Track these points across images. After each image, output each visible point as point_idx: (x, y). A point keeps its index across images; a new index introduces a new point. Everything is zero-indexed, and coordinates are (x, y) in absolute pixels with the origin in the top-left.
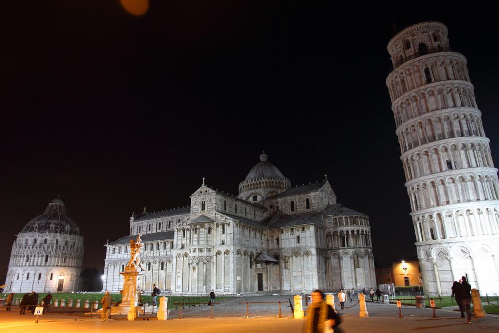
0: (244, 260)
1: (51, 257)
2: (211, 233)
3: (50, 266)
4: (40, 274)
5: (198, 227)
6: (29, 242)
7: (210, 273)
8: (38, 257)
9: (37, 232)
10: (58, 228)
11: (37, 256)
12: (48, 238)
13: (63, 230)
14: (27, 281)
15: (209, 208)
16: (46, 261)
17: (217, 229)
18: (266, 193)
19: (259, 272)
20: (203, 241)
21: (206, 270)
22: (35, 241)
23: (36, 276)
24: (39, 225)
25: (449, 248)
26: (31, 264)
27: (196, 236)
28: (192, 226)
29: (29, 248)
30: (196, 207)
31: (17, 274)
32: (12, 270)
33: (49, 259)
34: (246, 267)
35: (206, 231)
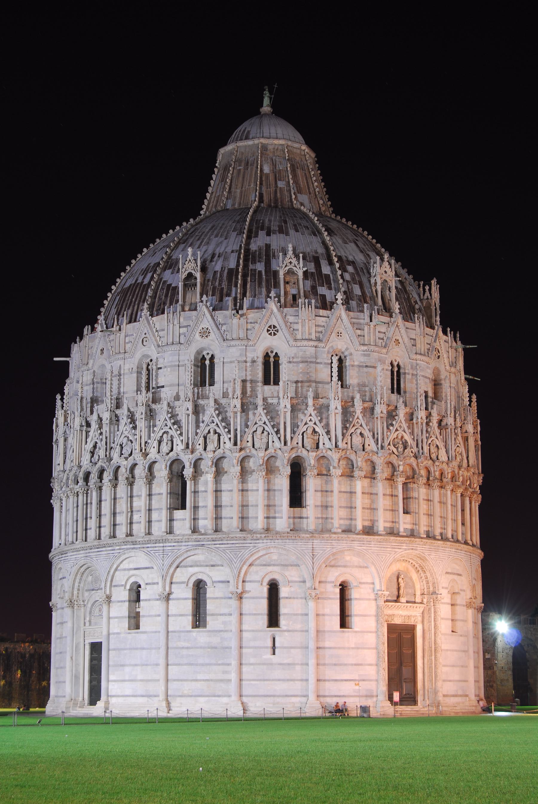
1: (324, 473)
3: (324, 530)
4: (273, 589)
6: (164, 378)
8: (244, 473)
9: (203, 309)
10: (326, 281)
11: (232, 469)
12: (280, 344)
13: (357, 290)
14: (200, 636)
16: (296, 499)
22: (204, 371)
23: (248, 605)
24: (204, 269)
26: (206, 523)
29: (132, 419)
31: (122, 595)
32: (85, 569)
33: (311, 484)
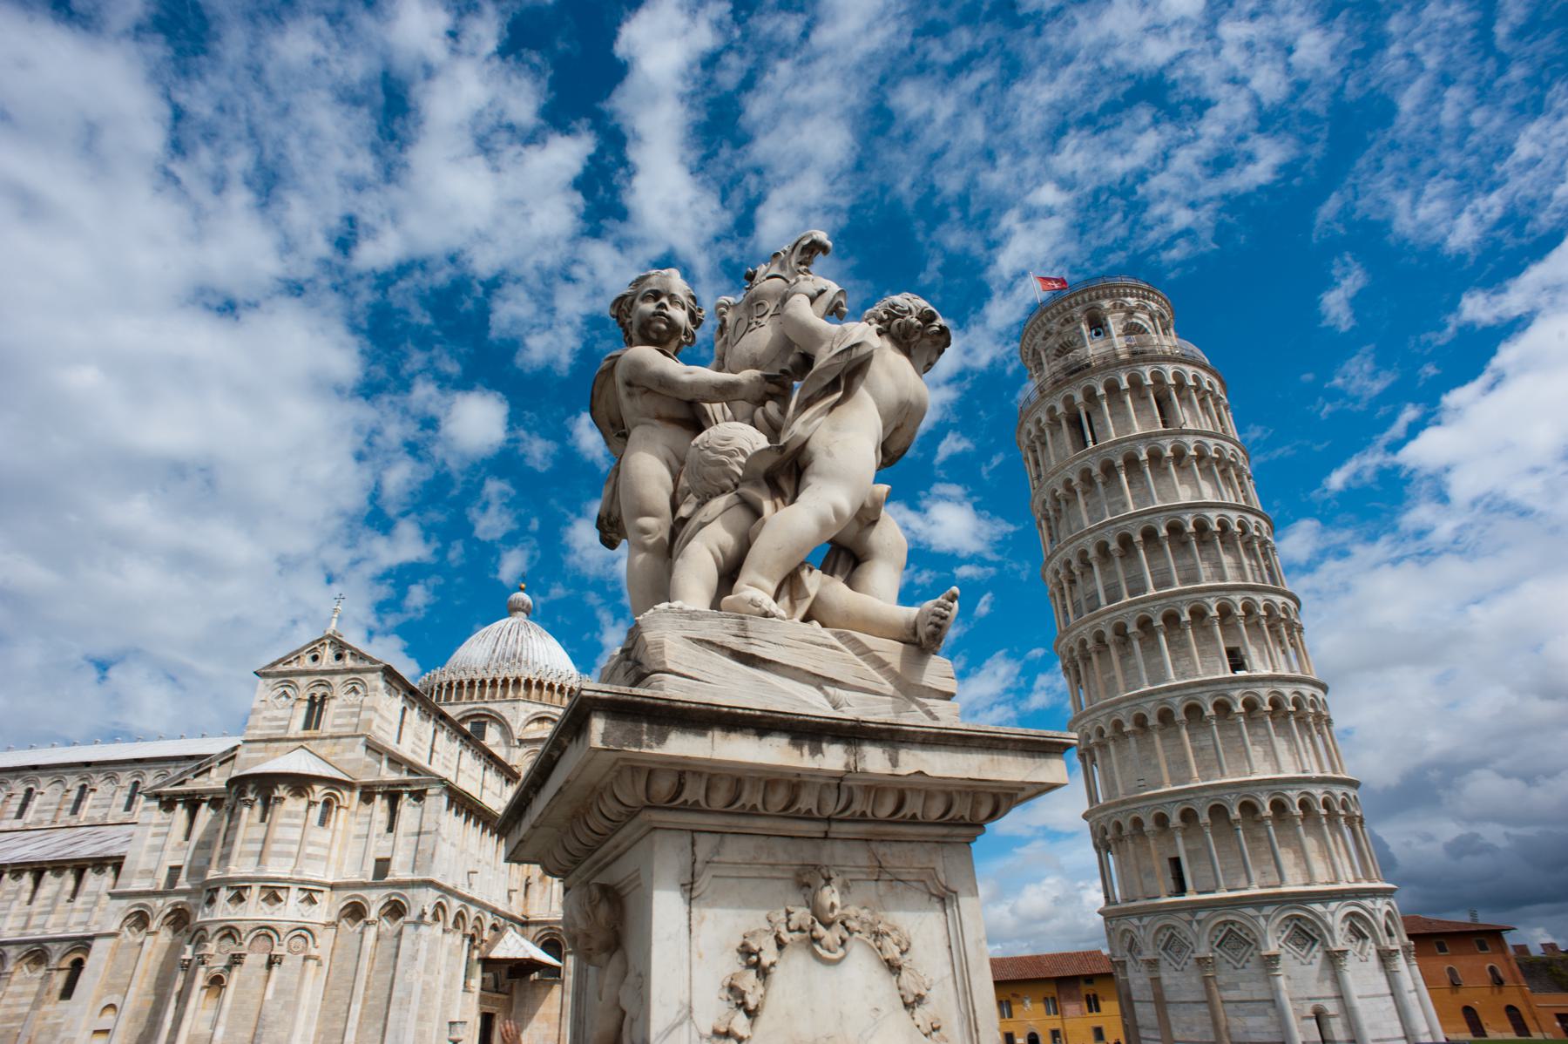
0: (450, 953)
2: (332, 824)
5: (277, 794)
7: (292, 1007)
15: (338, 721)
17: (365, 809)
18: (523, 717)
19: (488, 1009)
20: (289, 855)
21: (277, 992)
25: (1262, 921)
27: (259, 832)
28: (251, 787)
30: (280, 713)
34: (448, 986)
35: (316, 812)
